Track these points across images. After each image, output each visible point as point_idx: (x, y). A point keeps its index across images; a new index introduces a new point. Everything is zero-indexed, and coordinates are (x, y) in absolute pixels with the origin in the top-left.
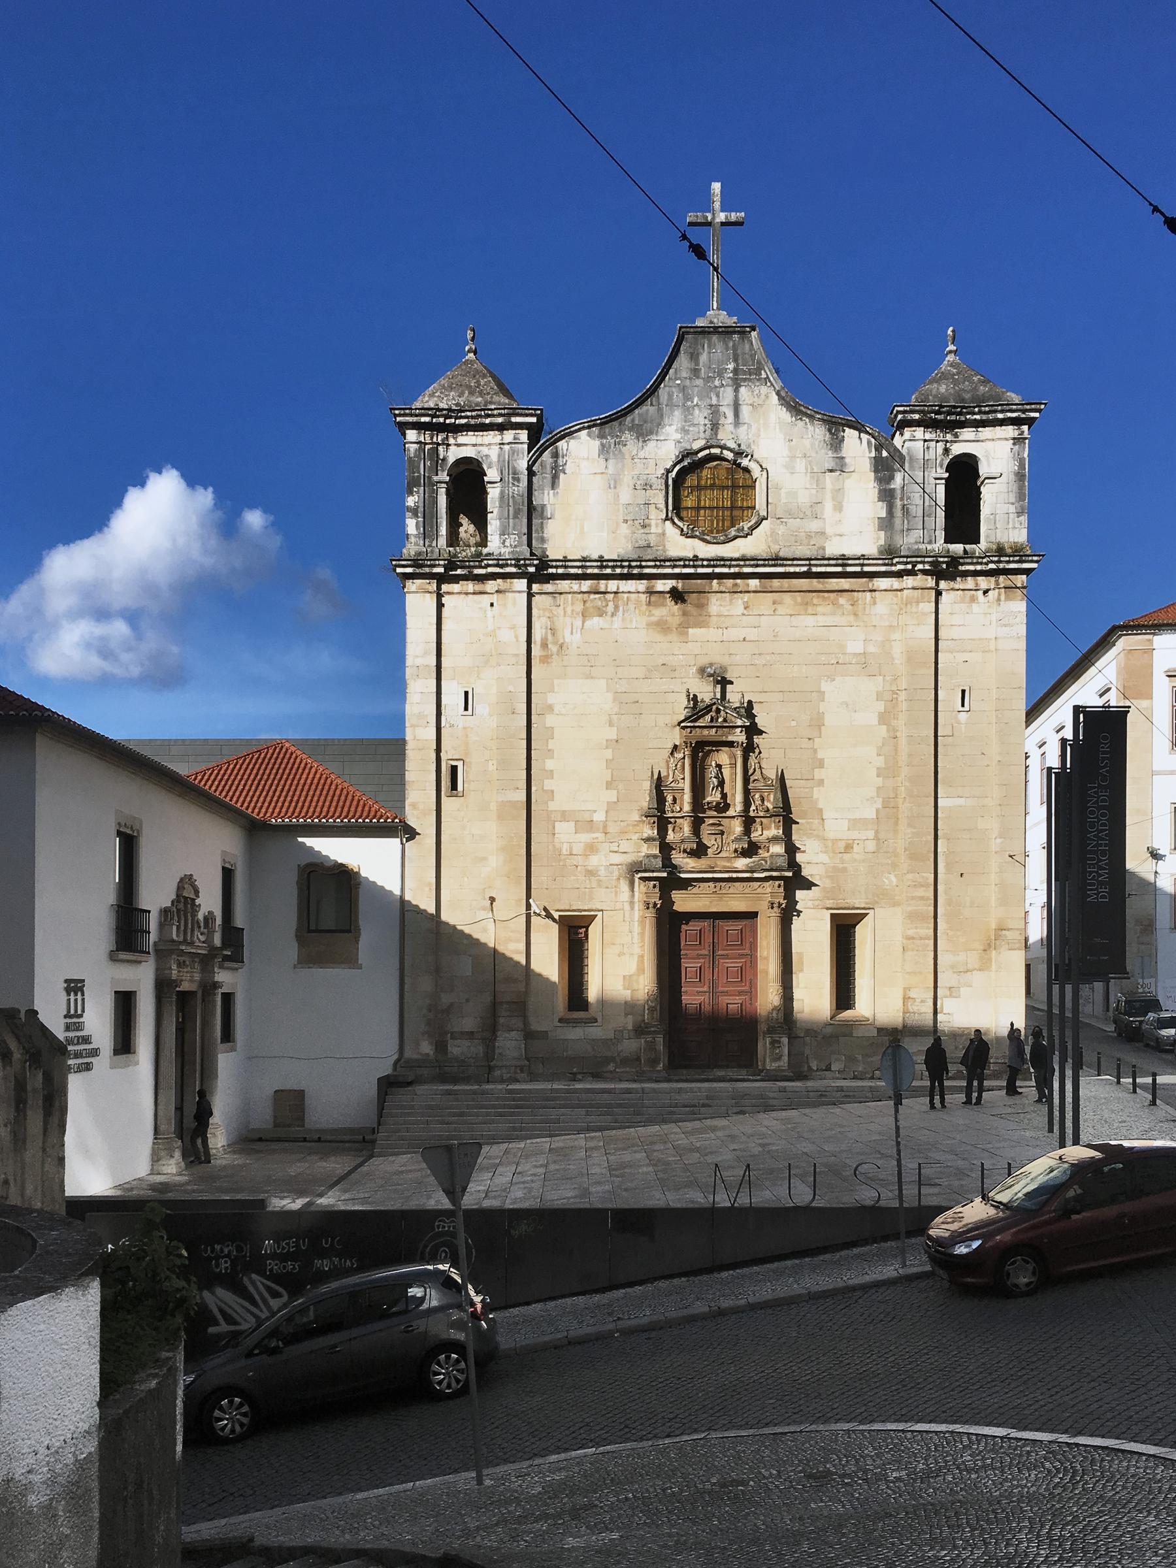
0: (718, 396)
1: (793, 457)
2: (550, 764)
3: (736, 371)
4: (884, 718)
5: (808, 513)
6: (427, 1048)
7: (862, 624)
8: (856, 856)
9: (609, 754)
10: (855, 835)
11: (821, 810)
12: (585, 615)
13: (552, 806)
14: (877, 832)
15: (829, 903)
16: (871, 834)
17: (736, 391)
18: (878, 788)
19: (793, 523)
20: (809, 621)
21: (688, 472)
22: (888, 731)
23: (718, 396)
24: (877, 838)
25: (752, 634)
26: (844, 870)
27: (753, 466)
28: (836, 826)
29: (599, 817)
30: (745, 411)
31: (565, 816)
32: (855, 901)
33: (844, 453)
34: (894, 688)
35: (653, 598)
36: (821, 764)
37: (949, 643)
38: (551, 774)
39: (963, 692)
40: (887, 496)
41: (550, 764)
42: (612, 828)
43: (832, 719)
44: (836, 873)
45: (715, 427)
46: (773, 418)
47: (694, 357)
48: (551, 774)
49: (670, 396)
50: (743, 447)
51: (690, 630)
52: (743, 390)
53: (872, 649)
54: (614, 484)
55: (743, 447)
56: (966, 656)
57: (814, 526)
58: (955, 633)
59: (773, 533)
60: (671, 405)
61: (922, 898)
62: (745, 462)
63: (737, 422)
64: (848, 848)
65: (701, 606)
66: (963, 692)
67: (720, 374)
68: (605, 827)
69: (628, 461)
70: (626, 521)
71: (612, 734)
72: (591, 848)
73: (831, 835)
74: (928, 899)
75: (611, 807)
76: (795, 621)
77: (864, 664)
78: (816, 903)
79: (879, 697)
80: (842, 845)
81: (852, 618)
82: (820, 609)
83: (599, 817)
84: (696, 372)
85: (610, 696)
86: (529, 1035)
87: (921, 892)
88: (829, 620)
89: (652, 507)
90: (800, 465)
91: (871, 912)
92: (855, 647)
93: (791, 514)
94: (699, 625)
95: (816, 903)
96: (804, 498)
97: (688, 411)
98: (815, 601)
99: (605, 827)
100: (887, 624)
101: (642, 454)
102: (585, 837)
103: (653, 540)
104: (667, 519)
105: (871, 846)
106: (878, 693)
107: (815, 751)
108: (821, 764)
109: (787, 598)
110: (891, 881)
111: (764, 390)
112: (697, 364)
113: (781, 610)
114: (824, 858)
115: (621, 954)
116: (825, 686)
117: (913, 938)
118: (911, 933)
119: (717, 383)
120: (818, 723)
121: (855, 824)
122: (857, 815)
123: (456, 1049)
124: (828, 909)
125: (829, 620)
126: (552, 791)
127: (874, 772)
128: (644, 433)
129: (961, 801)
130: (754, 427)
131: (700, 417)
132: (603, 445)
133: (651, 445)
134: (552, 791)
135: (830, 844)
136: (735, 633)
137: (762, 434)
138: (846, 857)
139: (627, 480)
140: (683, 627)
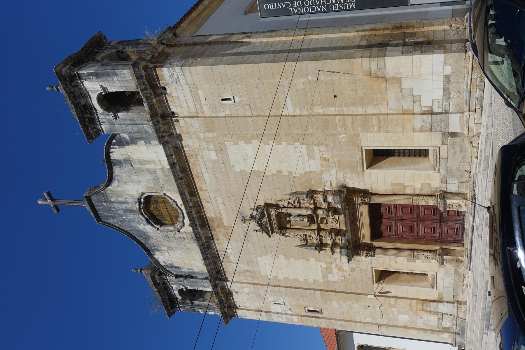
0: (119, 210)
1: (132, 181)
2: (301, 279)
3: (106, 202)
4: (248, 142)
5: (155, 175)
7: (200, 152)
8: (330, 155)
9: (292, 259)
10: (317, 156)
11: (306, 173)
12: (230, 262)
13: (321, 280)
14: (314, 145)
15: (360, 169)
16: (315, 148)
17: (114, 202)
18: (288, 144)
19: (162, 182)
20: (206, 176)
21: (155, 220)
22: (254, 139)
23: (119, 210)
24: (318, 145)
25: (220, 201)
26: (339, 161)
27: (143, 197)
28: (314, 165)
30: (120, 199)
31: (325, 277)
32: (358, 157)
34: (230, 136)
35: (215, 238)
36: (280, 172)
37: (198, 108)
38: (306, 280)
39: (223, 100)
40: (133, 141)
41: (301, 279)
42: (329, 260)
44: (341, 166)
45: (131, 211)
46: (119, 189)
47: (107, 217)
48: (306, 280)
49: (127, 226)
50: (136, 201)
51: (225, 225)
52: (112, 200)
53: (212, 147)
54: (170, 248)
55: (136, 201)
56: (202, 99)
57: (160, 173)
58: (191, 105)
59: (168, 190)
60: (131, 226)
61: (353, 123)
62: (142, 200)
64: (325, 159)
65: (213, 220)
66: (223, 100)
67: (110, 208)
68: (328, 263)
69: (158, 243)
70: (185, 245)
71: (282, 257)
72: (340, 269)
73: (319, 168)
74: (353, 119)
75: (318, 260)
76: (208, 181)
77: (221, 150)
78: (360, 176)
79: (236, 144)
80: (324, 163)
81: (199, 157)
82: (199, 171)
83: (324, 265)
85: (264, 257)
86: (441, 301)
87: (349, 123)
88: (203, 167)
89: (176, 236)
90: (135, 178)
91: (364, 148)
92: (213, 155)
93: (158, 182)
94: (222, 221)
95: (360, 176)
96: (149, 177)
97: (130, 220)
98: (196, 173)
99: (328, 263)
100: (197, 140)
101: (154, 238)
102: (335, 271)
103: (189, 236)
104: (179, 231)
105: (323, 148)
106: (234, 144)
107: (273, 175)
108: (280, 172)
109: (198, 185)
110: (344, 137)
111: (108, 192)
112: (109, 216)
113: (204, 187)
114: (333, 172)
115: (396, 262)
116: (238, 169)
117: (380, 127)
118: (376, 129)
119: (114, 210)
121: (311, 156)
122: (306, 157)
123: (447, 323)
124: (363, 170)
125: (203, 167)
126: (314, 280)
130: (125, 196)
131: (131, 216)
132: (157, 251)
133: (149, 234)
134: (314, 280)
135: (324, 168)
136: (221, 207)
137: (128, 193)
138: (331, 160)
139: (167, 243)
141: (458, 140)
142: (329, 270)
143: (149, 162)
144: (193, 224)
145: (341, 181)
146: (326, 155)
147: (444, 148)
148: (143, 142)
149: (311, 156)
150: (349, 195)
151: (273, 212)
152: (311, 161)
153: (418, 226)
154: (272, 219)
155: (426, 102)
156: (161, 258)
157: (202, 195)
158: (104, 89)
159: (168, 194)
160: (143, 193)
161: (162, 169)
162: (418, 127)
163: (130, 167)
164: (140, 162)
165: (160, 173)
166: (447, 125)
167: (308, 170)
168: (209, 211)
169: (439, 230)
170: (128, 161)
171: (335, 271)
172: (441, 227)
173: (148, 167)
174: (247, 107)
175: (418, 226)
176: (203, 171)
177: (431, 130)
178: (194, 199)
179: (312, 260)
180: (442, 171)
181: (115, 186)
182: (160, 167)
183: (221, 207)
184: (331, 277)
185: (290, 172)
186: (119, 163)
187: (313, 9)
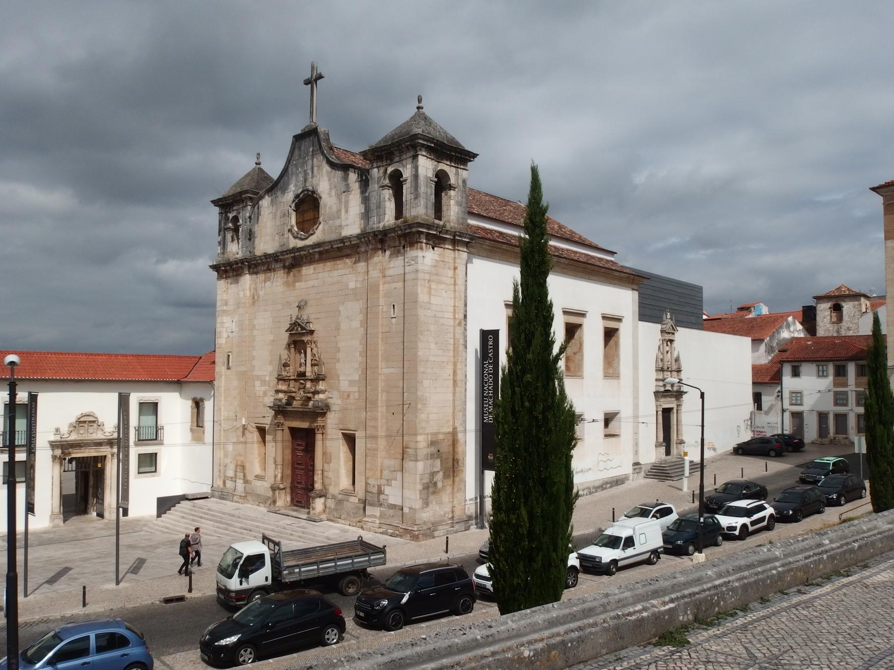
1: (331, 189)
6: (220, 483)
10: (350, 389)
15: (341, 427)
16: (356, 389)
19: (331, 222)
20: (335, 273)
24: (359, 391)
26: (347, 409)
28: (344, 385)
29: (267, 378)
30: (315, 169)
33: (349, 182)
43: (344, 326)
44: (344, 410)
45: (305, 180)
46: (325, 171)
47: (300, 148)
53: (358, 285)
57: (337, 222)
59: (324, 230)
60: (292, 174)
63: (313, 177)
64: (348, 396)
65: (300, 271)
71: (271, 337)
80: (346, 394)
84: (300, 155)
90: (333, 193)
92: (352, 285)
93: (330, 219)
96: (334, 209)
97: (297, 175)
102: (263, 388)
105: (357, 395)
107: (337, 343)
109: (328, 264)
114: (339, 402)
116: (341, 308)
118: (369, 446)
120: (338, 329)
121: (351, 383)
122: (351, 378)
123: (229, 484)
127: (358, 354)
128: (284, 190)
129: (392, 370)
136: (310, 283)
139: (278, 214)
140: (294, 282)
141: (361, 511)
142: (264, 383)
143: (347, 211)
144: (295, 250)
145: (333, 408)
146: (351, 397)
147: (357, 501)
148: (363, 211)
149: (351, 383)
150: (322, 411)
151: (305, 339)
152: (347, 382)
153: (302, 469)
154: (299, 337)
155: (387, 490)
156: (265, 202)
157: (320, 266)
158: (406, 180)
159: (321, 227)
160: (321, 198)
161: (340, 226)
162: (369, 481)
163: (343, 190)
164: (347, 202)
165: (337, 222)
166: (371, 505)
167: (341, 378)
168: (308, 271)
169: (300, 486)
170: (347, 190)
171: (263, 388)
172: (302, 488)
173: (343, 211)
174: (388, 330)
175: (302, 469)
176: (340, 271)
177: (366, 491)
178: (317, 256)
179: (270, 368)
180: (340, 497)
181: (326, 168)
182: (343, 224)
183: (310, 283)
184: (257, 383)
185: (338, 360)
186: (346, 178)
187: (486, 383)
